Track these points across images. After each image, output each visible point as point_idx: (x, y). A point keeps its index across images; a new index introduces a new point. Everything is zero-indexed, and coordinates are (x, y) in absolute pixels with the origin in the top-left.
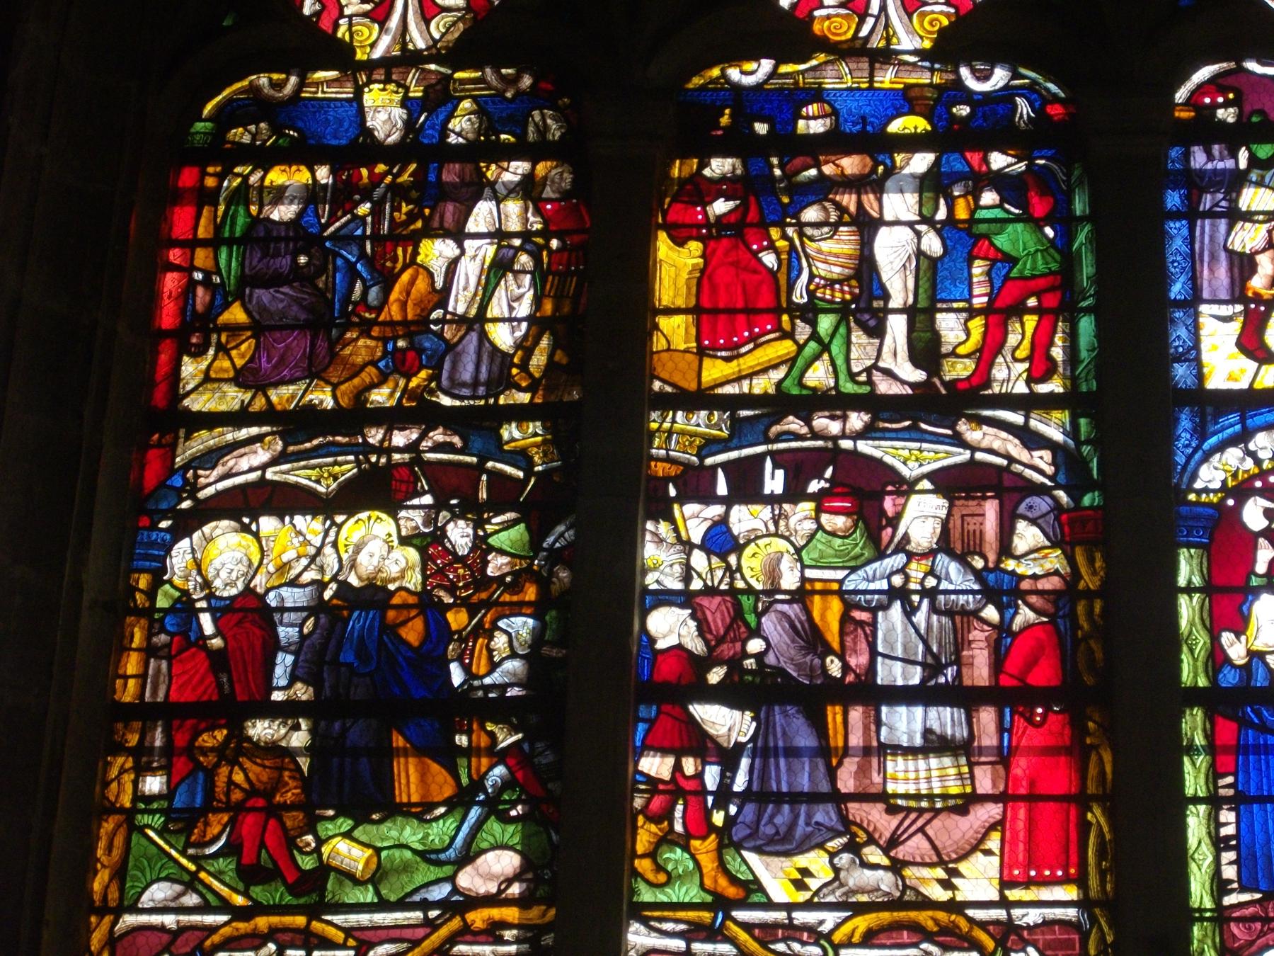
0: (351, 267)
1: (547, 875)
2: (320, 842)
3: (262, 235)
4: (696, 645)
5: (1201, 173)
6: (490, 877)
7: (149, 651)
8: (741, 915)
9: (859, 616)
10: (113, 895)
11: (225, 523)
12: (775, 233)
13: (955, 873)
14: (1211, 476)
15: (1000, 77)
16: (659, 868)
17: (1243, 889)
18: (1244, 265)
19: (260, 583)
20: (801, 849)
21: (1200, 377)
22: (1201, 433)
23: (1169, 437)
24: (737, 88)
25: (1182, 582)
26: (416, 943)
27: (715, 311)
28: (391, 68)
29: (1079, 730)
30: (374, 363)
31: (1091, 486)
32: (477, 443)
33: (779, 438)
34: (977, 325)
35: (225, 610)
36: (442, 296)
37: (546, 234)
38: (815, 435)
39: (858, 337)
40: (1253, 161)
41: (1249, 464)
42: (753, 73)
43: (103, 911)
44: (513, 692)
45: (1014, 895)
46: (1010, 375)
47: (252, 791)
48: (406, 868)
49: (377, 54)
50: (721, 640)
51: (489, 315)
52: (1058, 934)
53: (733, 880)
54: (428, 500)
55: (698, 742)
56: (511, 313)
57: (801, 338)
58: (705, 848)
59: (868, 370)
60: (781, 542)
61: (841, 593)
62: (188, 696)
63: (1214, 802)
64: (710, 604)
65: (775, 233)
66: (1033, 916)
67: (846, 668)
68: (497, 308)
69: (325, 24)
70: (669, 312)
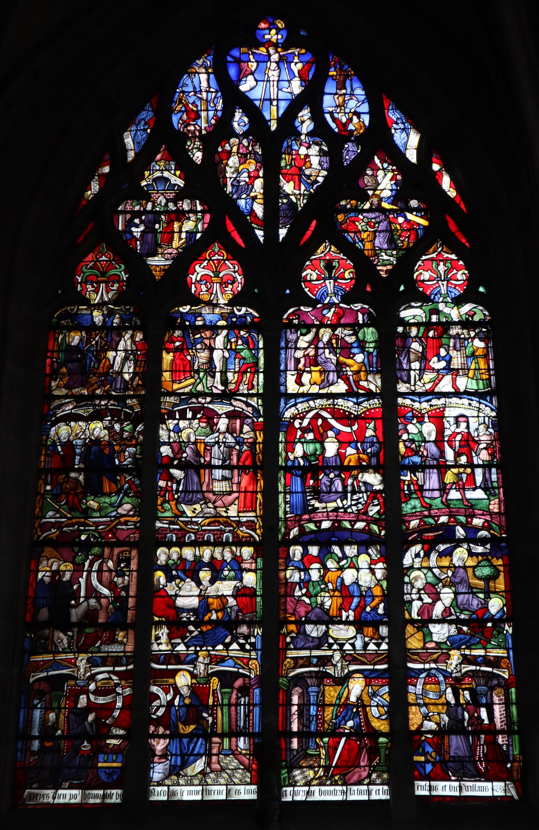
0: (91, 358)
1: (138, 509)
2: (87, 501)
4: (171, 455)
6: (125, 510)
7: (46, 455)
9: (208, 447)
10: (40, 515)
11: (63, 423)
13: (228, 509)
16: (163, 508)
17: (291, 513)
18: (297, 361)
19: (71, 438)
20: (194, 504)
21: (286, 390)
23: (279, 404)
24: (181, 313)
25: (280, 440)
26: (109, 525)
27: (176, 371)
28: (100, 306)
30: (97, 383)
31: (261, 416)
32: (121, 404)
34: (236, 375)
35: (63, 445)
37: (137, 350)
39: (209, 378)
41: (296, 411)
42: (185, 309)
45: (240, 514)
46: (243, 389)
47: (71, 489)
48: (106, 508)
49: (96, 302)
50: (177, 454)
51: (124, 371)
54: (109, 418)
55: (171, 478)
57: (196, 378)
58: (173, 503)
59: (211, 387)
60: (190, 430)
61: (204, 442)
63: (285, 493)
64: (175, 445)
65: (190, 351)
66: (244, 519)
67: (205, 461)
68: (125, 370)
69: (83, 293)
70: (166, 371)
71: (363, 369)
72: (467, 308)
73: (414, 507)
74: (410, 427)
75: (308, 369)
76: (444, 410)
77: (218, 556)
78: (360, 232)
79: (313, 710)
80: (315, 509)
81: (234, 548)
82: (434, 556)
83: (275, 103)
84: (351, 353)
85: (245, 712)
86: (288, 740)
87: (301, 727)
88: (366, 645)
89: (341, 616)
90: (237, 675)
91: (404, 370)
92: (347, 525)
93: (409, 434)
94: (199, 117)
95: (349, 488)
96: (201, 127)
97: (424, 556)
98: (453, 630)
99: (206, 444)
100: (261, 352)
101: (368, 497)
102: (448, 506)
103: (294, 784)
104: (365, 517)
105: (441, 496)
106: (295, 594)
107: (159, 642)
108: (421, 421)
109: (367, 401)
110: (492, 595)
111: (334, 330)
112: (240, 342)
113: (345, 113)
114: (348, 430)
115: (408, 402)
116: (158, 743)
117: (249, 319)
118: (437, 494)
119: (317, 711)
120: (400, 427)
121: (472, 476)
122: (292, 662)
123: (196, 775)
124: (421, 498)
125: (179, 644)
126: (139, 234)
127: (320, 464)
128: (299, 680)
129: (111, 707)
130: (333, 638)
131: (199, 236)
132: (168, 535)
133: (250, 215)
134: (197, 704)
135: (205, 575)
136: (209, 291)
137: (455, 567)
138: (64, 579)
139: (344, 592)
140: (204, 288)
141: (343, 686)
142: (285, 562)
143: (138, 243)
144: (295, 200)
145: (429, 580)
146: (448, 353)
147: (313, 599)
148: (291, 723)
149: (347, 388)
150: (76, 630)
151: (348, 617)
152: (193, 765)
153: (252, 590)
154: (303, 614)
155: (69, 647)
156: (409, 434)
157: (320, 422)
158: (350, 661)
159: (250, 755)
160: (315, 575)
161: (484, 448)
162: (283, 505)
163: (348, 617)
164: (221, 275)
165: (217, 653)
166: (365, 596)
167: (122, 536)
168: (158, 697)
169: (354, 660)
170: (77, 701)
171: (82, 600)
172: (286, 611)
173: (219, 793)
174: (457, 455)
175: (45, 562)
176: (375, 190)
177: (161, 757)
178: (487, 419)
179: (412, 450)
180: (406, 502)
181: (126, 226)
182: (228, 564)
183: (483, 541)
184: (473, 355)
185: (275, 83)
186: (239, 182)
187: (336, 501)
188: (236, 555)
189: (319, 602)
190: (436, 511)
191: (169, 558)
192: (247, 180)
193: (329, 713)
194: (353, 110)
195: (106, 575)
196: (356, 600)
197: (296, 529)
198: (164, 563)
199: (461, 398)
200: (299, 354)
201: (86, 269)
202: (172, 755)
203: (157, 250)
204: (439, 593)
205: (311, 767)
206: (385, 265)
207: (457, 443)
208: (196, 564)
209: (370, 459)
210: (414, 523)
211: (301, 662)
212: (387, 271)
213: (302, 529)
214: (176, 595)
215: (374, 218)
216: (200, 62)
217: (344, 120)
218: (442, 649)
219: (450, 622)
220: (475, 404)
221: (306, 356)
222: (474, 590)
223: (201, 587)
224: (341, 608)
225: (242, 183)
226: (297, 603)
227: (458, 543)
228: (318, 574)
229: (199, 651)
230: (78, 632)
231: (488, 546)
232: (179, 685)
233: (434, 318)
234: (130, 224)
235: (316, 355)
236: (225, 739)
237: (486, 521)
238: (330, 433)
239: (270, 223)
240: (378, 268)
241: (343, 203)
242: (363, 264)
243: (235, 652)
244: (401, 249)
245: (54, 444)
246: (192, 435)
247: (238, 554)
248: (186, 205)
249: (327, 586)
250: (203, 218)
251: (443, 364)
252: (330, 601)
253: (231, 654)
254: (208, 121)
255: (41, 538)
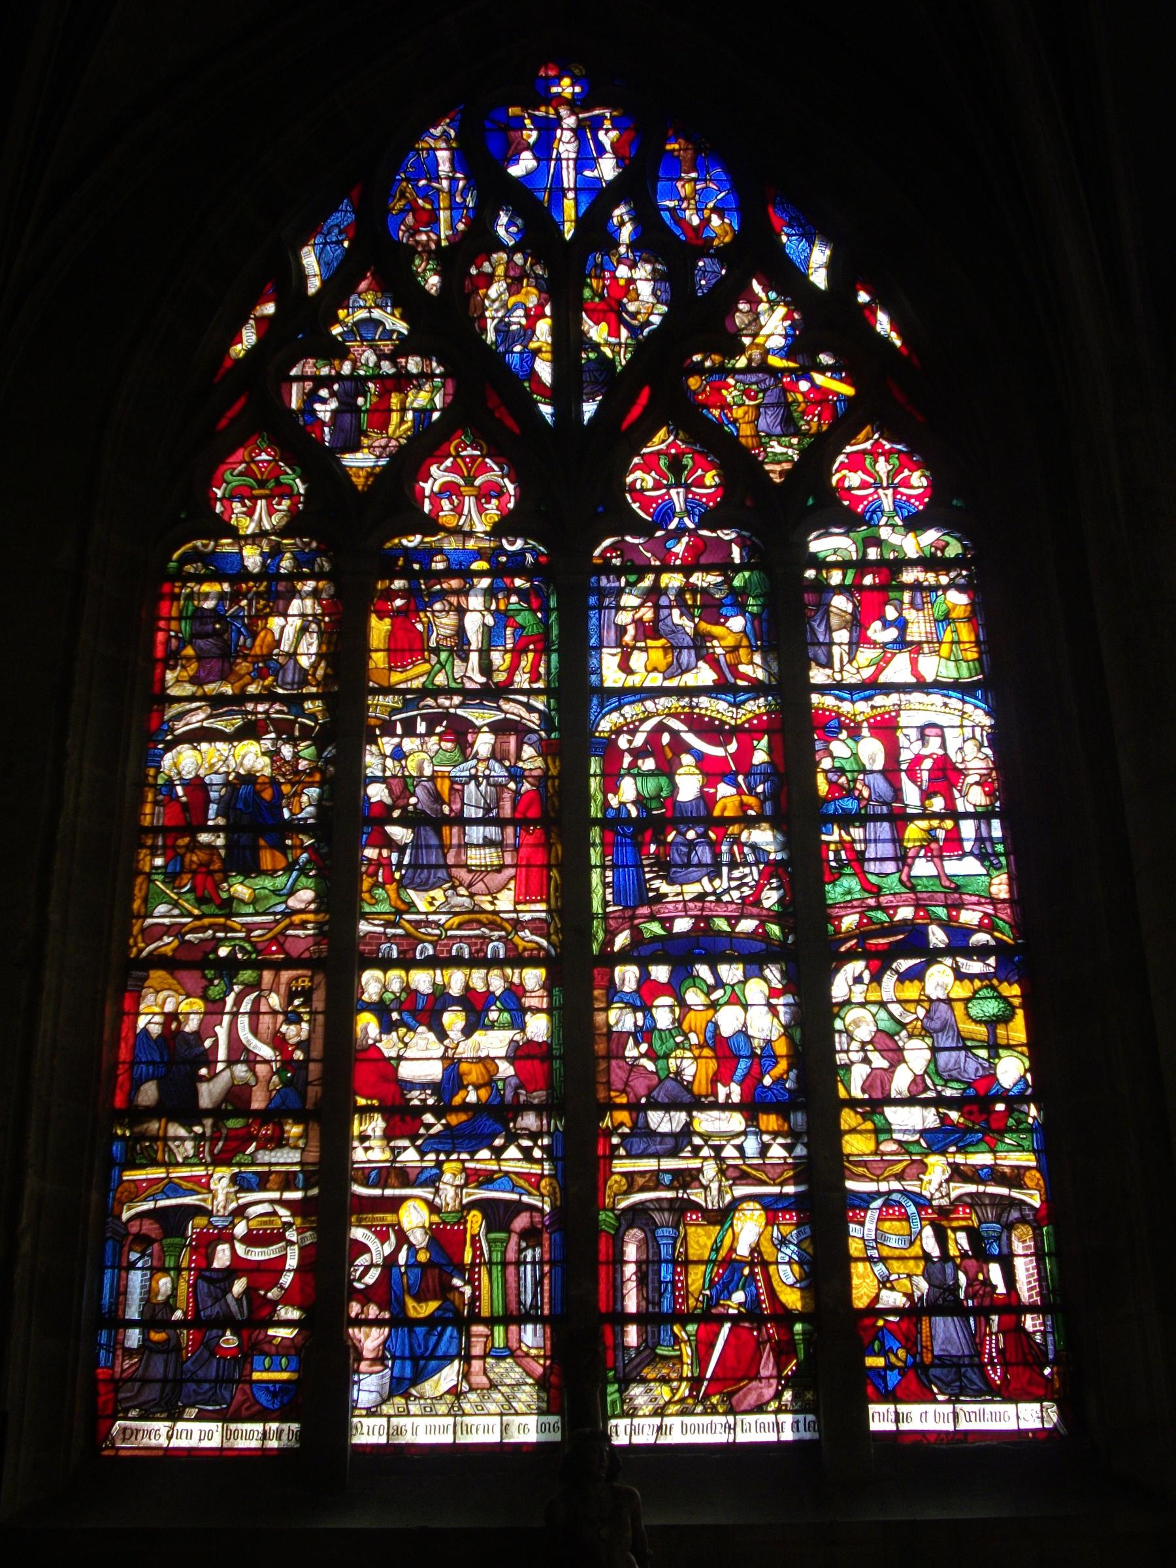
3: (200, 615)
5: (605, 588)
7: (156, 803)
8: (407, 917)
12: (422, 615)
14: (605, 725)
15: (519, 544)
16: (373, 897)
18: (622, 630)
19: (202, 772)
20: (432, 888)
21: (602, 681)
22: (602, 706)
24: (406, 548)
26: (271, 930)
27: (396, 651)
29: (548, 837)
31: (554, 729)
32: (294, 710)
33: (424, 707)
34: (508, 657)
35: (187, 784)
36: (278, 643)
37: (323, 615)
38: (439, 706)
39: (457, 662)
40: (628, 583)
41: (622, 720)
42: (413, 541)
43: (138, 917)
44: (310, 821)
45: (519, 907)
46: (522, 680)
47: (201, 865)
48: (266, 897)
49: (249, 532)
51: (300, 651)
52: (538, 924)
53: (404, 902)
54: (273, 735)
55: (389, 843)
56: (308, 651)
58: (392, 888)
60: (424, 754)
62: (173, 824)
63: (604, 867)
64: (394, 782)
65: (422, 615)
66: (528, 917)
67: (451, 810)
69: (226, 517)
71: (745, 642)
72: (931, 536)
73: (849, 892)
74: (837, 747)
75: (642, 644)
76: (898, 715)
77: (480, 987)
78: (730, 407)
79: (666, 1273)
80: (660, 898)
81: (509, 971)
82: (889, 980)
83: (571, 195)
84: (721, 616)
85: (534, 1276)
86: (618, 1329)
87: (644, 1303)
88: (764, 1148)
89: (715, 1093)
90: (518, 1207)
91: (820, 644)
92: (722, 925)
93: (833, 758)
94: (437, 220)
95: (725, 858)
96: (439, 236)
97: (871, 981)
98: (929, 1118)
99: (453, 780)
100: (553, 617)
101: (760, 873)
102: (912, 889)
103: (632, 1414)
104: (755, 911)
105: (899, 870)
106: (627, 1054)
107: (367, 1144)
108: (855, 734)
109: (754, 699)
110: (1002, 1052)
111: (688, 576)
112: (514, 599)
113: (698, 210)
114: (718, 752)
115: (829, 701)
116: (367, 1336)
117: (529, 558)
118: (890, 867)
119: (674, 1273)
120: (818, 745)
122: (624, 1181)
123: (441, 1397)
124: (861, 874)
125: (405, 1148)
126: (328, 415)
127: (669, 815)
128: (638, 1215)
129: (276, 1267)
130: (700, 1135)
131: (436, 416)
132: (383, 947)
133: (529, 380)
134: (443, 1261)
135: (454, 1020)
136: (458, 510)
137: (930, 1000)
138: (187, 1029)
139: (724, 1051)
140: (446, 504)
141: (722, 1226)
142: (607, 995)
143: (326, 430)
144: (609, 354)
145: (882, 1025)
146: (901, 614)
147: (661, 1063)
148: (623, 1297)
149: (715, 677)
150: (208, 1122)
151: (728, 1096)
152: (436, 1378)
153: (545, 1047)
154: (642, 1090)
155: (196, 1155)
156: (833, 758)
157: (666, 738)
158: (734, 1179)
159: (545, 1357)
160: (663, 1018)
161: (977, 783)
162: (600, 890)
163: (728, 1096)
164: (477, 482)
165: (479, 1166)
166: (761, 1057)
167: (296, 949)
168: (365, 1249)
169: (743, 1177)
170: (210, 1258)
171: (220, 1066)
172: (609, 1086)
173: (487, 1429)
174: (926, 795)
175: (151, 998)
176: (755, 335)
177: (374, 1361)
178: (978, 730)
179: (841, 787)
180: (833, 882)
181: (304, 402)
182: (498, 998)
183: (982, 952)
184: (947, 619)
185: (571, 163)
186: (509, 324)
187: (699, 881)
188: (512, 983)
189: (673, 1068)
190: (890, 898)
191: (385, 988)
192: (524, 321)
193: (696, 1278)
194: (711, 205)
195: (265, 1021)
196: (743, 1064)
197: (627, 933)
198: (375, 998)
199: (928, 694)
200: (624, 618)
201: (232, 476)
202: (394, 1358)
203: (360, 441)
204: (901, 1050)
205: (665, 1380)
206: (779, 463)
207: (925, 775)
208: (436, 999)
209: (762, 803)
210: (849, 921)
211: (640, 1181)
212: (781, 473)
213: (636, 932)
214: (400, 1058)
215: (756, 383)
216: (437, 132)
217: (696, 221)
218: (910, 1154)
219: (925, 1103)
220: (955, 703)
221: (638, 622)
222: (969, 1043)
223: (446, 1042)
224: (714, 1080)
225: (514, 327)
226: (631, 1071)
227: (933, 956)
228: (670, 1016)
229: (443, 1162)
230: (214, 1125)
231: (992, 961)
232: (406, 1226)
233: (873, 553)
234: (311, 398)
235: (656, 619)
236: (496, 1329)
237: (986, 915)
238: (687, 759)
239: (566, 392)
240: (767, 467)
241: (697, 358)
242: (737, 462)
243: (512, 1163)
244: (805, 434)
245: (170, 784)
246: (426, 765)
247: (516, 980)
248: (413, 365)
249: (687, 1038)
250: (444, 385)
251: (892, 634)
252: (694, 1067)
253: (505, 1167)
254: (452, 226)
255: (144, 954)
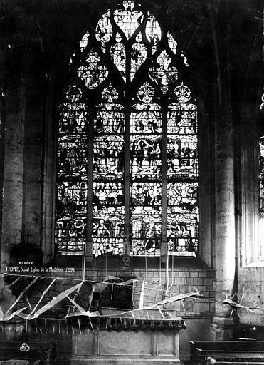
72: (190, 105)
121: (189, 162)
174: (185, 155)
248: (100, 68)
